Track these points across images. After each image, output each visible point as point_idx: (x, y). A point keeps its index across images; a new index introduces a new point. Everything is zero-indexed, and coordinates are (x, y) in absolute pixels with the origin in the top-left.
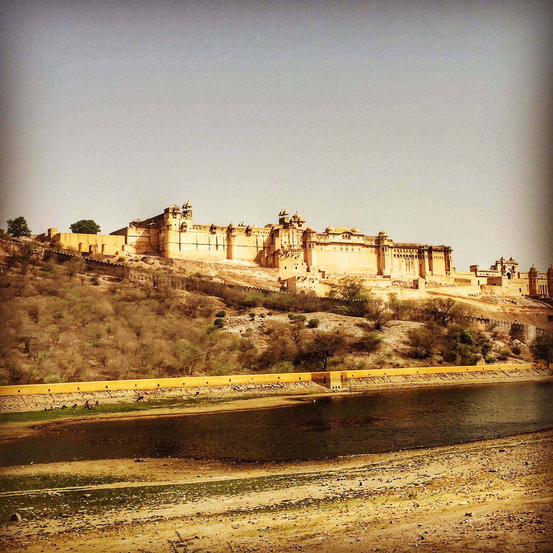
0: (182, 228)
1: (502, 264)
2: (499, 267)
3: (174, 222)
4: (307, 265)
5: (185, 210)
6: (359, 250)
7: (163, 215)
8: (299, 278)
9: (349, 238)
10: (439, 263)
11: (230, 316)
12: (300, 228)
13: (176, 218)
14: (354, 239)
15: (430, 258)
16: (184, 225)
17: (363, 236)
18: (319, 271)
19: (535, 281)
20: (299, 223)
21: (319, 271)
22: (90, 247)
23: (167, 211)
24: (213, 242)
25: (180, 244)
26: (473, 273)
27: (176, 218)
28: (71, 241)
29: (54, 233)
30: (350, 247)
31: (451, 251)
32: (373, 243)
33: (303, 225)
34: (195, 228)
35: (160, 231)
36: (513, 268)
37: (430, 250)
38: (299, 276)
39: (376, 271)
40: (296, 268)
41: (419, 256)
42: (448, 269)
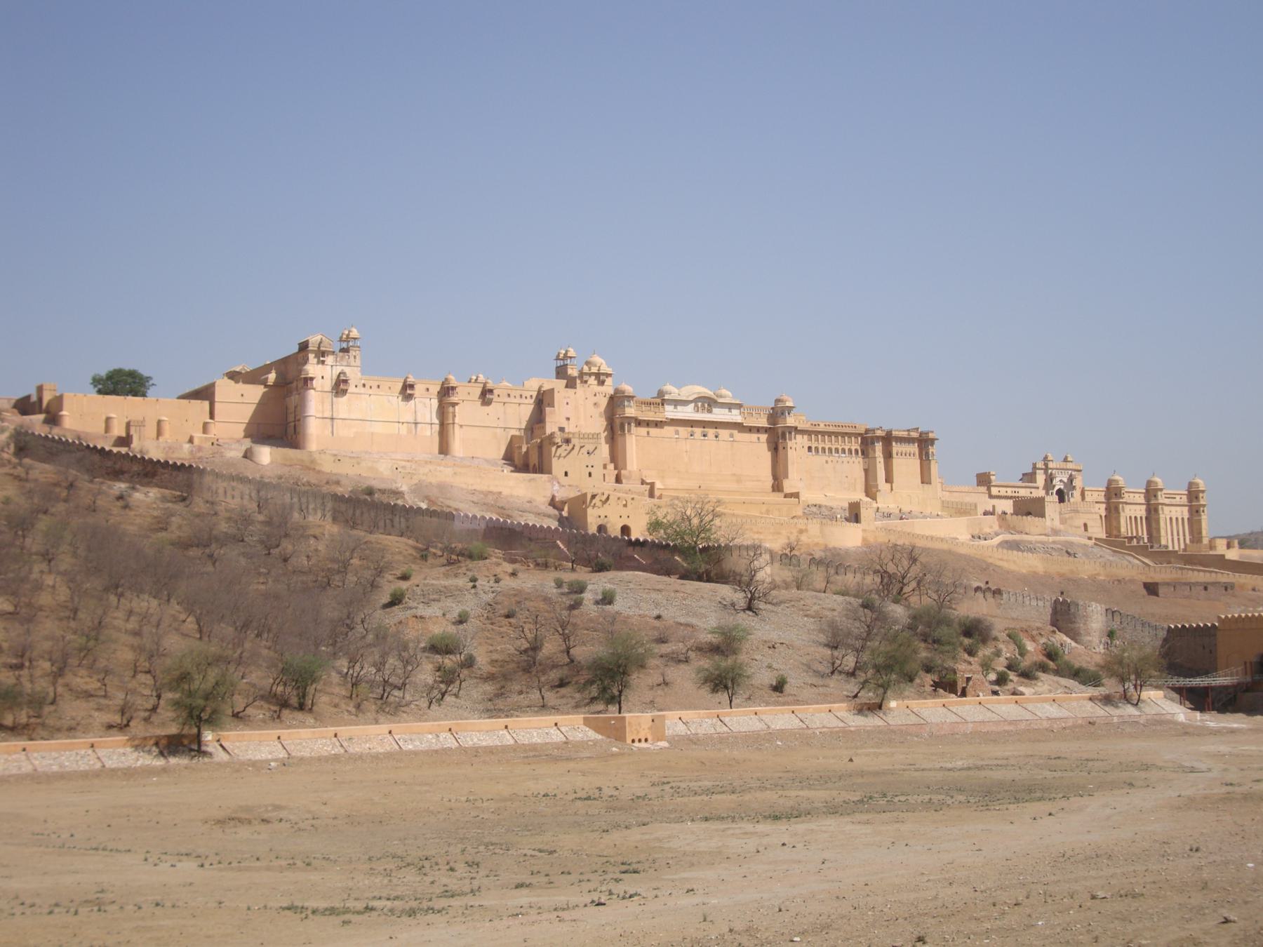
1: (1046, 469)
2: (1041, 478)
3: (320, 373)
4: (616, 468)
5: (344, 345)
6: (732, 436)
8: (594, 497)
9: (710, 411)
10: (906, 463)
11: (432, 577)
12: (601, 388)
13: (323, 362)
14: (719, 415)
15: (888, 456)
16: (342, 378)
18: (643, 482)
19: (1117, 509)
21: (643, 482)
22: (128, 425)
23: (304, 347)
26: (983, 489)
27: (323, 362)
28: (88, 417)
29: (47, 397)
31: (932, 441)
32: (763, 422)
33: (609, 381)
35: (289, 393)
36: (1071, 479)
37: (888, 439)
38: (595, 492)
39: (769, 481)
40: (590, 475)
41: (863, 453)
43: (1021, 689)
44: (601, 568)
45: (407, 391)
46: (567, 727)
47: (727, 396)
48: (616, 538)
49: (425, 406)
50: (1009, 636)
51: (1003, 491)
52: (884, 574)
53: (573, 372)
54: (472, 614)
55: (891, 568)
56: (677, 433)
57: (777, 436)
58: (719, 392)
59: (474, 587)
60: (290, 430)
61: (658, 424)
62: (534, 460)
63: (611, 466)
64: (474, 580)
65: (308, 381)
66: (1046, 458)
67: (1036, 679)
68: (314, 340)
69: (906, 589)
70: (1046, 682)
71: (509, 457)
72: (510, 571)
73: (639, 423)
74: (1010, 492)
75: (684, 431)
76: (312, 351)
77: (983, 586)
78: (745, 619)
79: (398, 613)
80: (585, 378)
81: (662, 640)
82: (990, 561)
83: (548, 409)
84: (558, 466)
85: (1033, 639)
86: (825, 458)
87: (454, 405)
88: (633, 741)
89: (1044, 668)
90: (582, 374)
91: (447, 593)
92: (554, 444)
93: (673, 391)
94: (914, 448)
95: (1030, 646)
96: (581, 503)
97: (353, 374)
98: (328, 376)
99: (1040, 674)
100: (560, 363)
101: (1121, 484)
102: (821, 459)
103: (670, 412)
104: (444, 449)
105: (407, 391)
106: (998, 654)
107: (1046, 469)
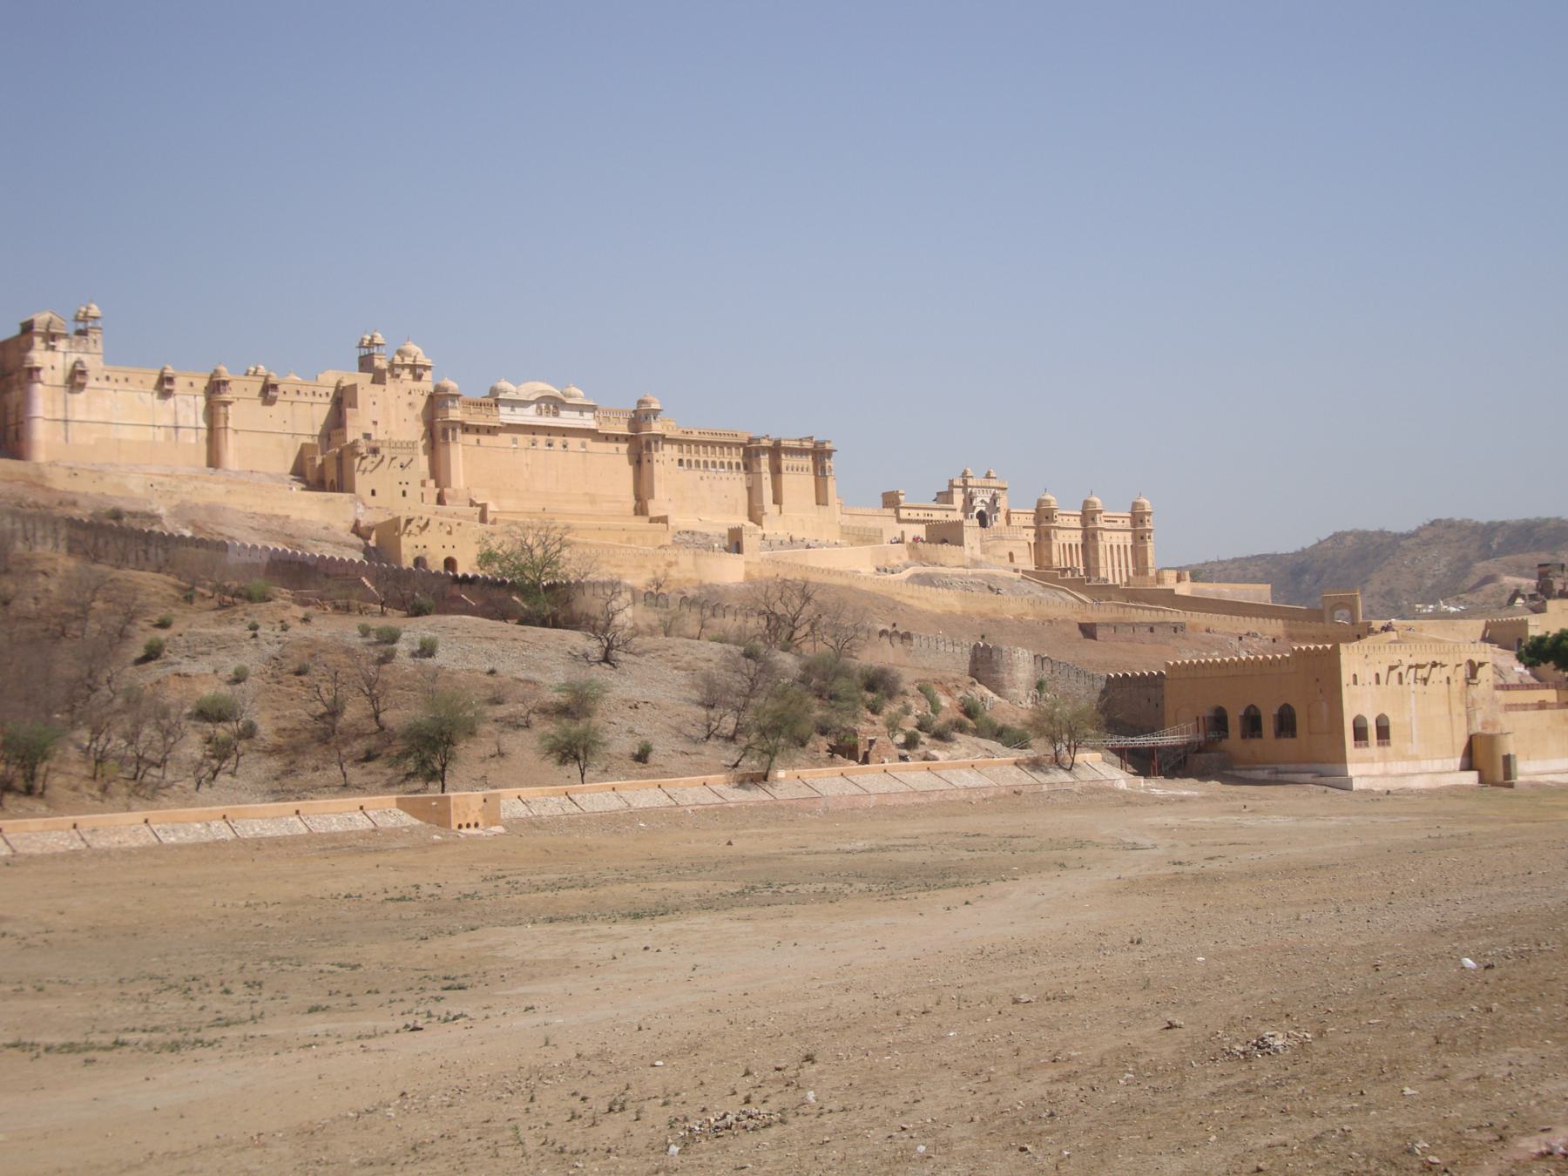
0: (75, 379)
1: (965, 487)
2: (958, 498)
3: (50, 362)
4: (437, 485)
5: (81, 326)
6: (584, 445)
7: (15, 340)
8: (409, 522)
9: (556, 415)
10: (798, 479)
11: (198, 623)
12: (417, 385)
14: (567, 419)
15: (776, 471)
16: (79, 368)
19: (1048, 535)
21: (472, 503)
23: (28, 328)
26: (890, 511)
27: (53, 348)
30: (558, 441)
31: (829, 453)
32: (622, 429)
33: (427, 375)
36: (994, 500)
37: (776, 451)
38: (411, 515)
39: (631, 502)
40: (404, 494)
43: (934, 753)
44: (418, 611)
45: (164, 386)
46: (377, 810)
47: (578, 395)
48: (438, 573)
49: (189, 406)
50: (920, 689)
51: (914, 514)
52: (770, 616)
53: (381, 363)
54: (252, 670)
55: (779, 609)
56: (515, 441)
57: (640, 446)
58: (567, 390)
59: (255, 636)
60: (11, 436)
61: (491, 431)
62: (331, 475)
63: (432, 483)
64: (254, 627)
65: (33, 372)
66: (964, 474)
67: (952, 740)
68: (41, 319)
69: (798, 634)
70: (964, 744)
71: (299, 472)
72: (301, 615)
73: (466, 429)
74: (922, 515)
75: (523, 439)
76: (39, 334)
77: (890, 629)
78: (601, 673)
79: (155, 670)
80: (397, 371)
81: (496, 701)
82: (898, 598)
83: (349, 411)
84: (362, 482)
85: (948, 692)
86: (699, 473)
87: (226, 404)
88: (460, 826)
89: (960, 727)
90: (392, 366)
92: (358, 454)
93: (510, 390)
94: (808, 461)
95: (945, 701)
96: (392, 529)
97: (93, 362)
99: (956, 735)
100: (364, 352)
101: (1054, 504)
102: (695, 474)
103: (506, 415)
104: (214, 460)
105: (164, 386)
106: (907, 711)
107: (965, 487)
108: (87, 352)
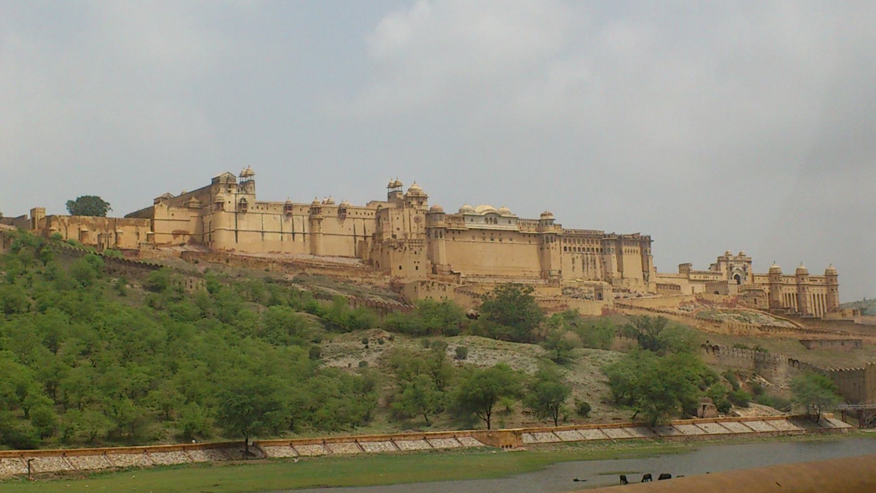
0: (242, 207)
2: (723, 267)
5: (244, 180)
13: (230, 191)
14: (502, 226)
15: (620, 253)
17: (517, 218)
20: (421, 199)
23: (216, 181)
24: (288, 228)
25: (236, 231)
26: (684, 275)
34: (260, 207)
36: (745, 268)
37: (620, 240)
40: (417, 268)
42: (645, 271)
43: (738, 412)
59: (367, 347)
61: (459, 231)
65: (220, 205)
67: (747, 407)
73: (447, 231)
91: (352, 352)
98: (233, 201)
100: (391, 190)
108: (247, 193)
